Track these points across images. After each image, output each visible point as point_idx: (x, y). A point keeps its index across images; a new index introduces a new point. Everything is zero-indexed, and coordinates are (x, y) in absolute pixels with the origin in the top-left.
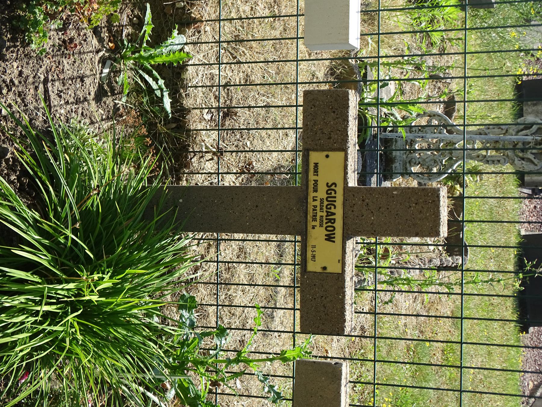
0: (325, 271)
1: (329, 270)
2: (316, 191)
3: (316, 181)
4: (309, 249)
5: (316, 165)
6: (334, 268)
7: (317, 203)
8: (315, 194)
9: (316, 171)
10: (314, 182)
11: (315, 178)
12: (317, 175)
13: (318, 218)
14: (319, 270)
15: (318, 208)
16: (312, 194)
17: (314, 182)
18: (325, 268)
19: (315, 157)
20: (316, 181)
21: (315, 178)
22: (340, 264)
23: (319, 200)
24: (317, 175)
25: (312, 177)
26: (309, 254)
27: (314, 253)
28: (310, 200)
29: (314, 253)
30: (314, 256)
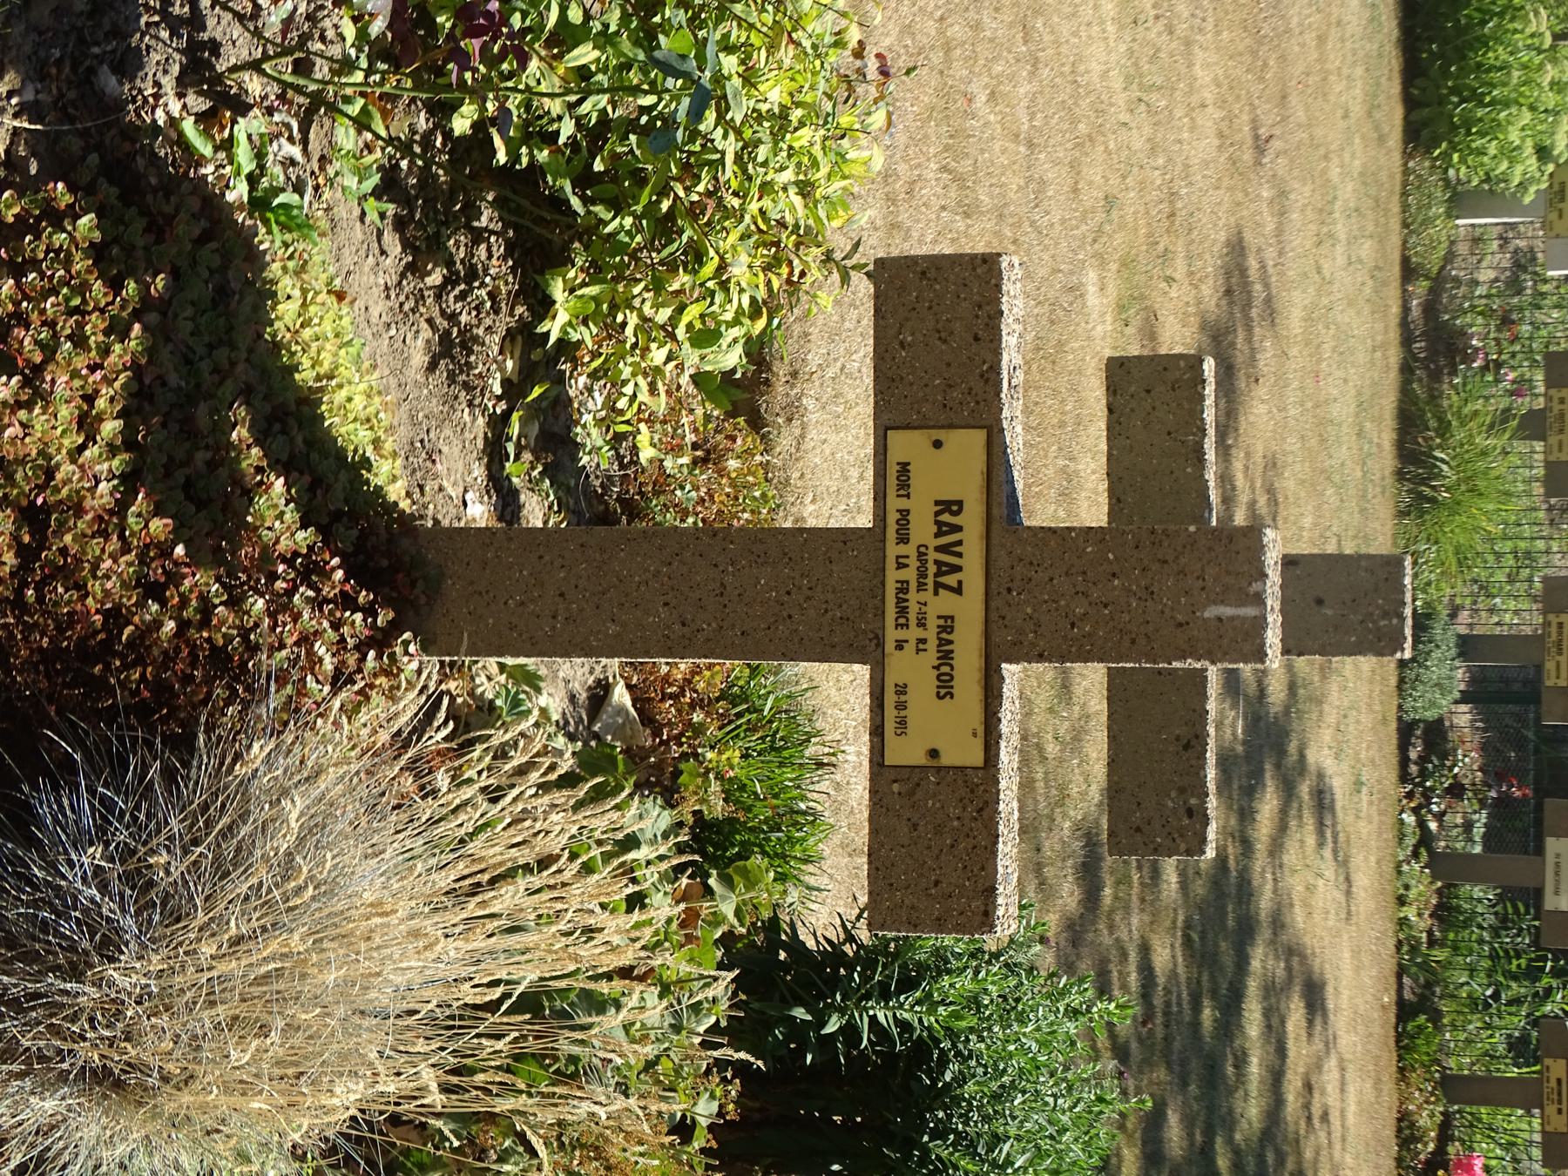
0: (934, 763)
1: (946, 760)
2: (903, 539)
3: (904, 513)
4: (890, 698)
5: (904, 468)
6: (964, 752)
7: (910, 574)
8: (902, 549)
9: (904, 485)
10: (898, 516)
11: (903, 504)
12: (908, 496)
13: (912, 616)
14: (919, 758)
15: (913, 585)
16: (893, 550)
17: (898, 516)
18: (934, 753)
19: (904, 444)
20: (904, 513)
21: (903, 504)
22: (979, 743)
23: (913, 563)
24: (908, 496)
25: (894, 503)
26: (890, 713)
27: (903, 713)
28: (891, 563)
29: (903, 713)
30: (902, 723)
